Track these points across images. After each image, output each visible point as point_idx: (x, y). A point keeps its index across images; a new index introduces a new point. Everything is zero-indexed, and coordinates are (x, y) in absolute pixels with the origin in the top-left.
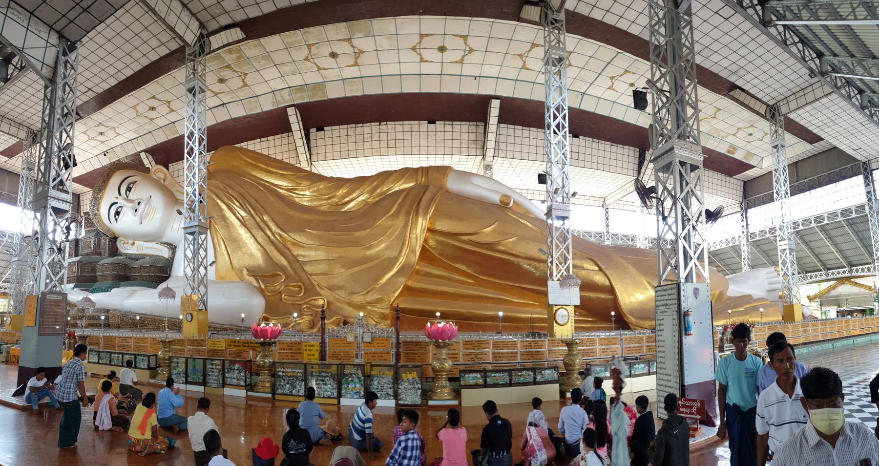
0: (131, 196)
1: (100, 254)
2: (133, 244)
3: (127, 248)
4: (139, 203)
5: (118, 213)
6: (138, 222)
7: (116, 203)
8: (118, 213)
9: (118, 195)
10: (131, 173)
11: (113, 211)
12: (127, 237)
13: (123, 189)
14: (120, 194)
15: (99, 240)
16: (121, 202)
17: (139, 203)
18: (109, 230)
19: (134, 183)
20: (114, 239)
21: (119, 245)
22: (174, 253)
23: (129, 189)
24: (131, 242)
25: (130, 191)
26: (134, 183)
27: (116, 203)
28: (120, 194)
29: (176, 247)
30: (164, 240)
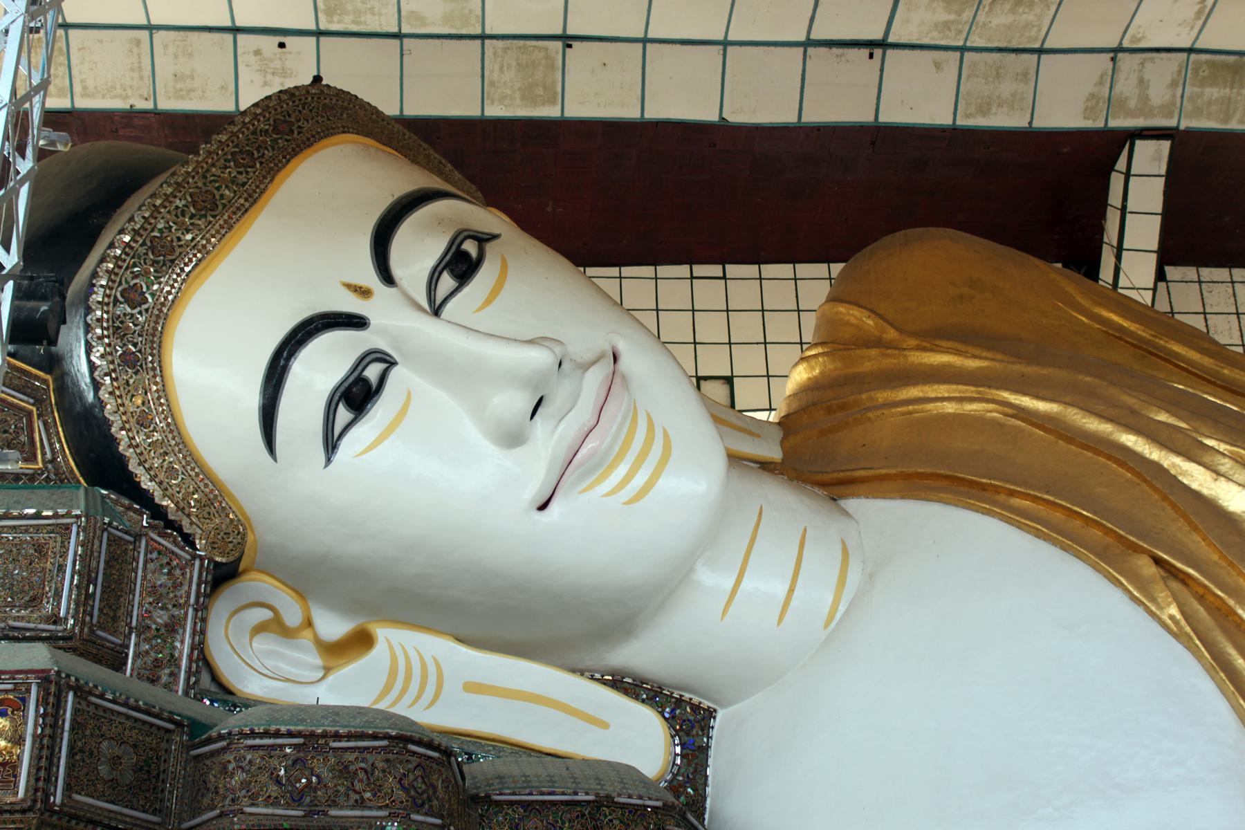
2: (361, 641)
5: (357, 395)
6: (533, 490)
7: (356, 322)
8: (357, 395)
9: (370, 278)
11: (321, 368)
12: (312, 577)
13: (418, 250)
14: (387, 277)
15: (120, 557)
18: (214, 498)
19: (483, 240)
23: (460, 264)
24: (333, 627)
27: (356, 322)
28: (387, 277)
30: (634, 655)
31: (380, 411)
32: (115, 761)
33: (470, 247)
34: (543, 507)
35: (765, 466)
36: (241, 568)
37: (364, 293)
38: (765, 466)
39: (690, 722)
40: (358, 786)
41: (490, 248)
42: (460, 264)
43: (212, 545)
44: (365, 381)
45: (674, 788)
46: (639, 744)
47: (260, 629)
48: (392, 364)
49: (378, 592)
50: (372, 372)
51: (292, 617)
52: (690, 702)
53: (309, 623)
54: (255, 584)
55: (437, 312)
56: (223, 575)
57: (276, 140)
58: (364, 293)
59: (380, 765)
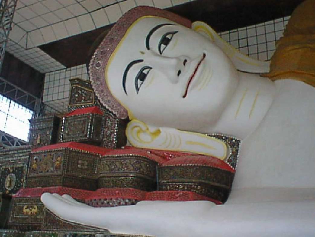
0: (168, 50)
1: (99, 144)
3: (142, 138)
4: (185, 61)
5: (142, 76)
7: (142, 61)
8: (142, 76)
10: (163, 21)
16: (149, 59)
17: (185, 61)
19: (173, 33)
20: (124, 123)
21: (131, 134)
22: (235, 154)
23: (165, 41)
24: (152, 129)
25: (166, 44)
26: (173, 33)
27: (142, 61)
28: (148, 48)
29: (238, 142)
31: (147, 79)
32: (82, 164)
33: (169, 37)
34: (184, 97)
35: (263, 75)
36: (130, 118)
37: (143, 53)
38: (263, 75)
39: (233, 144)
40: (124, 167)
41: (174, 35)
42: (165, 41)
43: (120, 114)
44: (144, 73)
45: (229, 161)
46: (219, 151)
47: (139, 132)
48: (151, 68)
49: (160, 121)
50: (145, 72)
51: (144, 128)
52: (234, 139)
53: (148, 129)
54: (134, 122)
55: (161, 53)
56: (127, 121)
57: (126, 23)
58: (143, 53)
59: (128, 162)
